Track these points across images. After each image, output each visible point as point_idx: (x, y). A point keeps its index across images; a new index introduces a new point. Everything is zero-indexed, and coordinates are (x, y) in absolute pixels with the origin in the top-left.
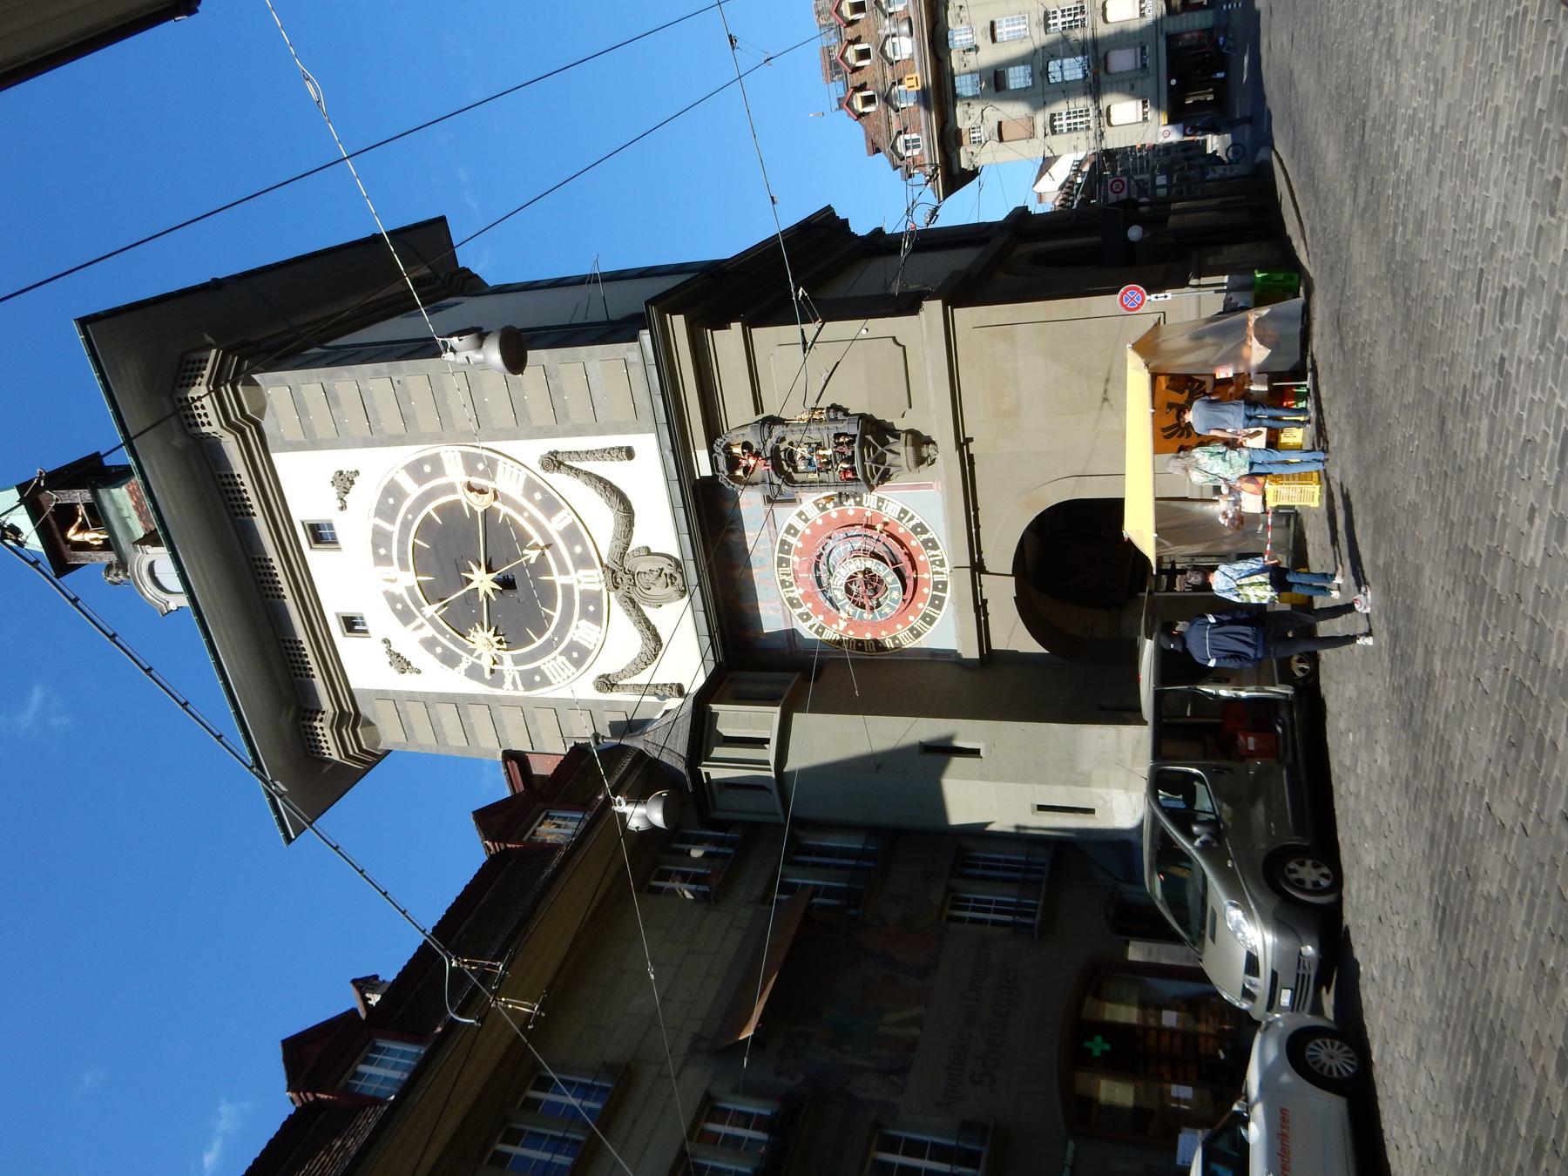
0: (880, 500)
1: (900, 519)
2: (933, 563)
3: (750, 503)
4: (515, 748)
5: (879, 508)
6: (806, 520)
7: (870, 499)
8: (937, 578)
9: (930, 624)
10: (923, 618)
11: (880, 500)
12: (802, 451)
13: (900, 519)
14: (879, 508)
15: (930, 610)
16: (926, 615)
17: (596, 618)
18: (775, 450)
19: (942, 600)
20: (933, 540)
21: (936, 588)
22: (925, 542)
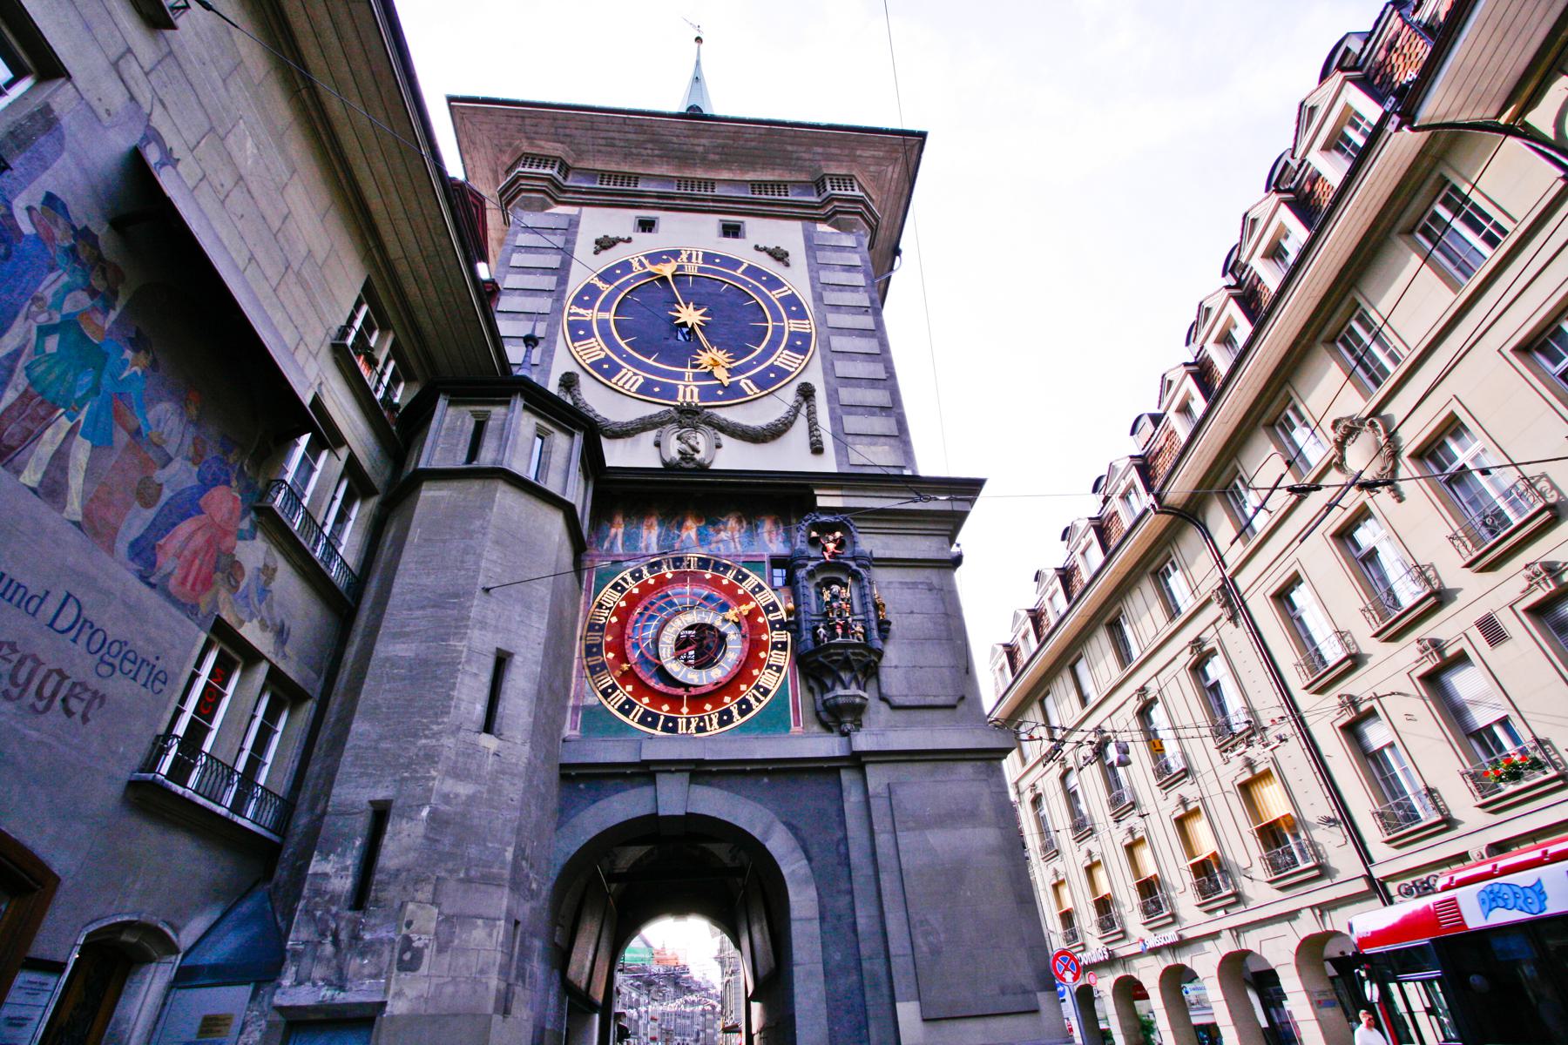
0: (779, 669)
1: (757, 687)
2: (702, 719)
3: (772, 541)
4: (503, 299)
5: (770, 667)
6: (753, 591)
7: (783, 659)
8: (682, 722)
9: (621, 709)
10: (628, 701)
11: (779, 669)
12: (845, 593)
13: (757, 687)
14: (770, 667)
15: (639, 710)
16: (633, 705)
17: (646, 388)
18: (845, 569)
19: (653, 725)
21: (667, 719)
22: (728, 712)
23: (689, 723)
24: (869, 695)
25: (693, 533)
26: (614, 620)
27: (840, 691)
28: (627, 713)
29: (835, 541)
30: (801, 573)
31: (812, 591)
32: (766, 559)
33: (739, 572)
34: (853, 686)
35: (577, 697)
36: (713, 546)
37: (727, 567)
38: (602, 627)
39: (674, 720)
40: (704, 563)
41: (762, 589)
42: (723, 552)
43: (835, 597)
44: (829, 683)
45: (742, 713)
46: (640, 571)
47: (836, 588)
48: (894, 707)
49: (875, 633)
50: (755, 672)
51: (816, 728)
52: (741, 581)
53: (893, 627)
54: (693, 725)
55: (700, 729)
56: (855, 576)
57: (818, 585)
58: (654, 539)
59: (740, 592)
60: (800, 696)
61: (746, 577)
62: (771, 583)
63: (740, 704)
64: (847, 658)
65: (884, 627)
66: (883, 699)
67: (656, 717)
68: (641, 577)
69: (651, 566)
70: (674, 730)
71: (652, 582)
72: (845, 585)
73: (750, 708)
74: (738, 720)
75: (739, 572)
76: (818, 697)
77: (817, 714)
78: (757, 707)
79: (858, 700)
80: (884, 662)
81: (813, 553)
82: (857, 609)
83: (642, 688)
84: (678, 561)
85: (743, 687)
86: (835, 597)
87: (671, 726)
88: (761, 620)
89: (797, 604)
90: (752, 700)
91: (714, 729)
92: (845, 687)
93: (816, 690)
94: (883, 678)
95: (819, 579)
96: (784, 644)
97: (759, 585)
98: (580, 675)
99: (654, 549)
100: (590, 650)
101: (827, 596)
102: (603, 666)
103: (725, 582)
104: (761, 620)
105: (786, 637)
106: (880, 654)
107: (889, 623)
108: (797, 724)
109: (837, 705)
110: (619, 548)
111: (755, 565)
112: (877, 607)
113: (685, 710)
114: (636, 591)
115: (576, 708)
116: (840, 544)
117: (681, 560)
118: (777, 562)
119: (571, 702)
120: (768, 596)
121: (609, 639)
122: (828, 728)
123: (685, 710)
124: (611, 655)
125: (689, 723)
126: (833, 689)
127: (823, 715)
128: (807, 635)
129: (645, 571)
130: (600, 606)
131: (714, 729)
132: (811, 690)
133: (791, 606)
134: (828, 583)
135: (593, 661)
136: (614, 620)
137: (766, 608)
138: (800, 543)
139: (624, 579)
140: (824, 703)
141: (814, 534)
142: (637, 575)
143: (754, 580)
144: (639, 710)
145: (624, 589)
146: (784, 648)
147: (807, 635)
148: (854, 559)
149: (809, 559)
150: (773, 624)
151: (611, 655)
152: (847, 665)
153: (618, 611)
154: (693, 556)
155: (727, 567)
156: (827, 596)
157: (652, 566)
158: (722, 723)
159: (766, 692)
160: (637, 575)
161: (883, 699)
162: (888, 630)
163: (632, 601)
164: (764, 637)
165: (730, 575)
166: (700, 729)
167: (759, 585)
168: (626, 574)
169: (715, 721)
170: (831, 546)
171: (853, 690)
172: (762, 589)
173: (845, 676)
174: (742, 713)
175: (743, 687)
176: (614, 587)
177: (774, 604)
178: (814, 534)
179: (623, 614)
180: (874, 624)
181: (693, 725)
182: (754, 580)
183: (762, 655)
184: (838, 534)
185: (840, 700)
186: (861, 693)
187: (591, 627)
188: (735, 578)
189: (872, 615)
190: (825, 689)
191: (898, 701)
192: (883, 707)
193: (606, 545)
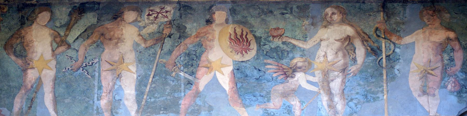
25: (225, 79)
58: (129, 89)
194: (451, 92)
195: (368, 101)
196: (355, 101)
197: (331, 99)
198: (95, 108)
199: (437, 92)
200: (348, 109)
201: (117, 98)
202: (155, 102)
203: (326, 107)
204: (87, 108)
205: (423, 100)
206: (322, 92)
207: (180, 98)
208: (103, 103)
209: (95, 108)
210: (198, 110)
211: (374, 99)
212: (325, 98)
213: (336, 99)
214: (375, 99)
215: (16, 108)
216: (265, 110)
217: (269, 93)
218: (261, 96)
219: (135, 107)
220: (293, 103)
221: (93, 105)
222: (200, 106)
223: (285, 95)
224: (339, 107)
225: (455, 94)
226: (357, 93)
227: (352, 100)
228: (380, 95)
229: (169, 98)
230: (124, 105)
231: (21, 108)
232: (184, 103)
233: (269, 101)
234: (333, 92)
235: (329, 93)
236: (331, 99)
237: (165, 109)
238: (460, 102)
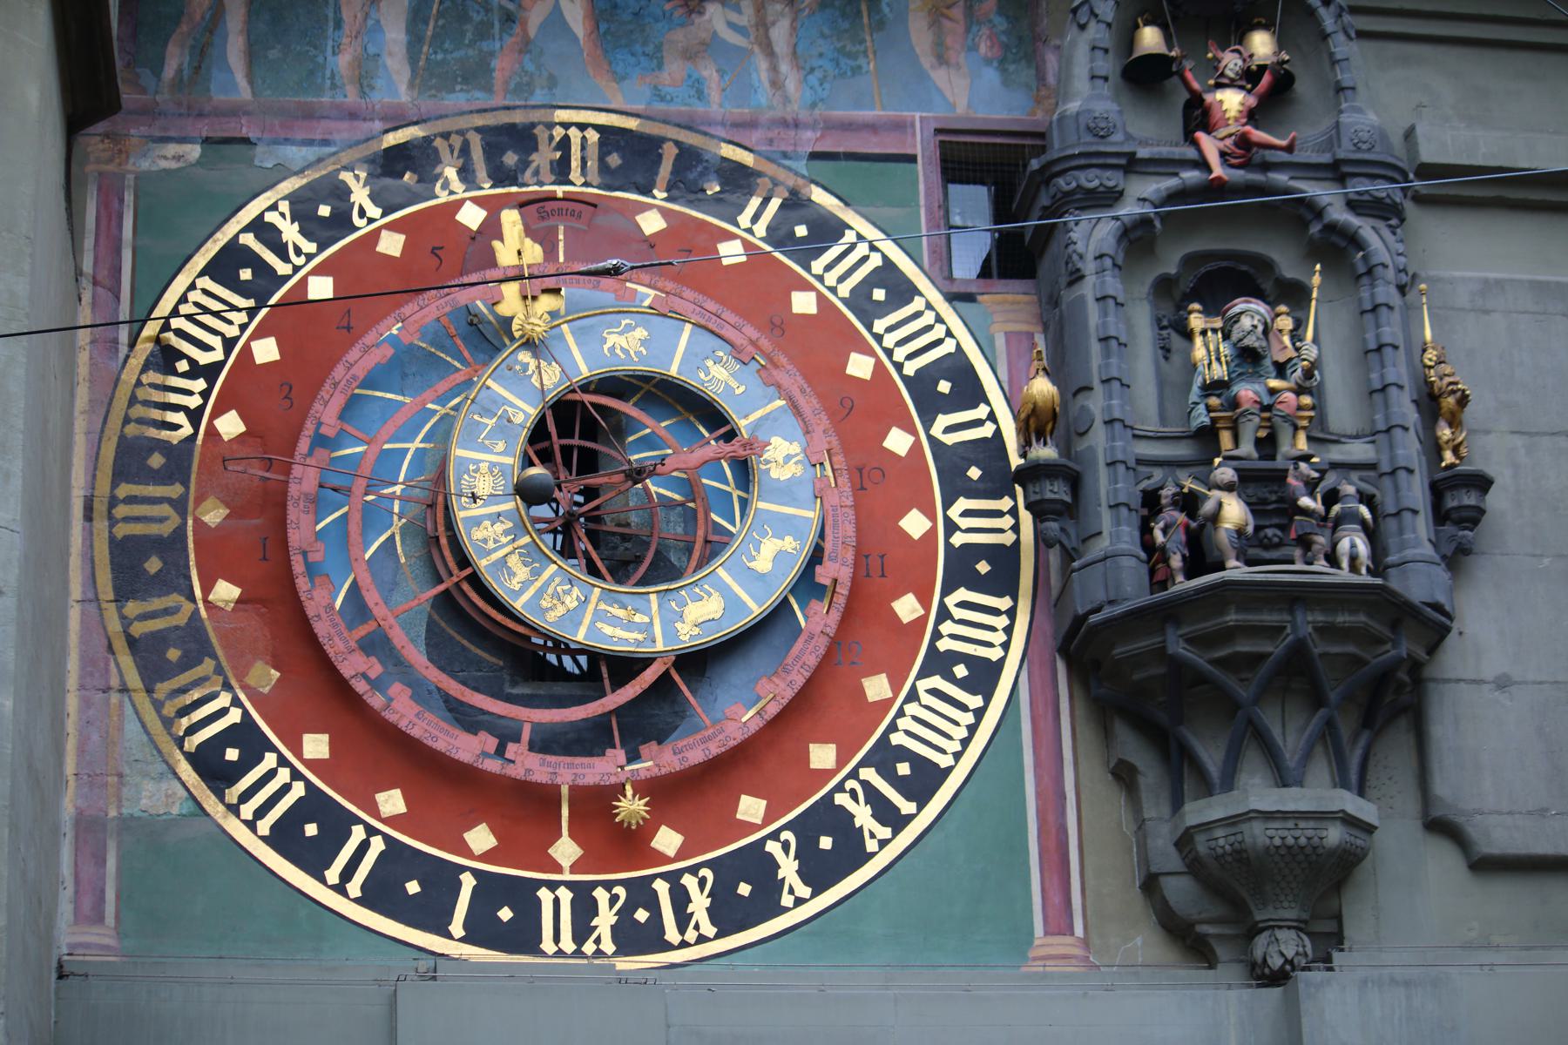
0: (983, 676)
1: (884, 757)
2: (641, 893)
5: (939, 663)
6: (860, 301)
7: (1000, 631)
8: (554, 905)
9: (284, 838)
11: (983, 676)
13: (884, 757)
14: (939, 663)
15: (365, 848)
16: (337, 826)
19: (433, 916)
20: (767, 902)
22: (758, 865)
23: (585, 909)
24: (1387, 813)
26: (230, 425)
27: (1258, 792)
28: (314, 859)
29: (1249, 77)
30: (1091, 234)
31: (1141, 320)
32: (921, 144)
33: (795, 204)
34: (1320, 771)
35: (91, 779)
36: (674, 69)
37: (739, 180)
38: (178, 459)
39: (523, 896)
40: (632, 158)
41: (903, 291)
42: (716, 104)
43: (1249, 357)
44: (1211, 756)
45: (819, 873)
46: (341, 194)
47: (1250, 313)
48: (1487, 866)
49: (1422, 526)
50: (876, 687)
51: (1144, 942)
52: (807, 252)
53: (1495, 500)
54: (605, 920)
55: (633, 938)
56: (1337, 249)
57: (1164, 287)
59: (804, 303)
60: (1074, 795)
61: (827, 231)
62: (942, 272)
63: (806, 829)
64: (1299, 650)
65: (1458, 500)
66: (1442, 827)
67: (442, 880)
68: (341, 222)
69: (392, 163)
70: (523, 937)
71: (392, 244)
72: (1295, 295)
73: (853, 852)
74: (801, 904)
75: (795, 204)
76: (1155, 809)
77: (1150, 885)
78: (885, 849)
79: (1334, 835)
80: (1454, 659)
81: (1149, 131)
82: (1342, 411)
83: (377, 748)
84: (507, 149)
85: (822, 756)
86: (1249, 357)
87: (507, 919)
88: (898, 442)
89: (1073, 387)
90: (863, 815)
91: (697, 941)
92: (1283, 778)
93: (1150, 774)
94: (1441, 730)
95: (1170, 264)
96: (1005, 559)
97: (886, 273)
98: (97, 683)
99: (396, 82)
100: (137, 567)
101: (1208, 353)
102: (195, 642)
103: (731, 253)
104: (898, 442)
105: (1001, 522)
106: (1434, 626)
107: (1482, 483)
108: (1059, 923)
109: (1240, 857)
110: (234, 80)
111: (861, 165)
112: (1430, 402)
113: (566, 850)
114: (321, 288)
115: (89, 828)
116: (1274, 93)
117: (523, 138)
118: (964, 158)
119: (68, 806)
120: (932, 326)
121: (214, 515)
122: (1191, 944)
123: (566, 850)
124: (226, 592)
125: (585, 909)
126: (1228, 783)
127: (1179, 890)
128: (1114, 535)
129: (360, 195)
130: (166, 358)
131: (697, 941)
132: (1124, 775)
133: (1042, 387)
134: (1220, 282)
135: (155, 614)
136: (230, 425)
137: (921, 384)
138: (1084, 89)
139: (259, 227)
140: (1184, 842)
141: (1150, 38)
142: (324, 215)
143: (866, 241)
144: (365, 848)
145: (267, 278)
146: (1003, 578)
147: (1114, 535)
148: (1337, 172)
149: (1132, 165)
150: (952, 461)
151: (226, 592)
152: (1297, 675)
153: (241, 384)
154: (579, 119)
155: (739, 180)
156: (1208, 353)
157: (399, 166)
158: (728, 916)
159: (925, 780)
160: (324, 215)
161: (1442, 827)
162: (1473, 518)
163: (312, 334)
164: (914, 524)
165: (756, 218)
166: (633, 938)
167: (886, 273)
168: (271, 205)
169: (699, 904)
170: (1231, 101)
171: (1318, 793)
172: (903, 291)
173: (1290, 731)
174: (819, 873)
175: (822, 756)
176: (224, 268)
177: (958, 368)
178: (1150, 38)
179: (277, 405)
180: (1416, 492)
181: (605, 920)
182: (866, 241)
183: (907, 607)
184: (1261, 44)
185: (1259, 835)
186: (1349, 802)
187: (131, 460)
188: (779, 235)
189: (1409, 448)
190: (1183, 772)
191: (1500, 838)
192: (1442, 860)
193: (175, 60)
194: (988, 62)
195: (843, 75)
196: (818, 74)
197: (774, 69)
198: (328, 73)
199: (962, 59)
200: (808, 93)
201: (372, 50)
202: (444, 61)
203: (767, 84)
204: (312, 73)
205: (939, 76)
206: (756, 49)
207: (492, 54)
208: (342, 62)
209: (328, 73)
210: (528, 84)
211: (852, 69)
212: (763, 65)
213: (784, 67)
214: (857, 70)
215: (169, 72)
216: (655, 87)
217: (659, 48)
218: (644, 54)
219: (406, 74)
220: (705, 73)
221: (324, 67)
222: (532, 75)
223: (689, 55)
224: (791, 85)
225: (995, 64)
226: (821, 55)
227: (812, 70)
228: (862, 61)
229: (471, 52)
230: (385, 67)
231: (180, 71)
232: (502, 66)
233: (660, 66)
234: (777, 49)
235: (770, 52)
236: (774, 69)
237: (466, 80)
238: (1006, 82)
